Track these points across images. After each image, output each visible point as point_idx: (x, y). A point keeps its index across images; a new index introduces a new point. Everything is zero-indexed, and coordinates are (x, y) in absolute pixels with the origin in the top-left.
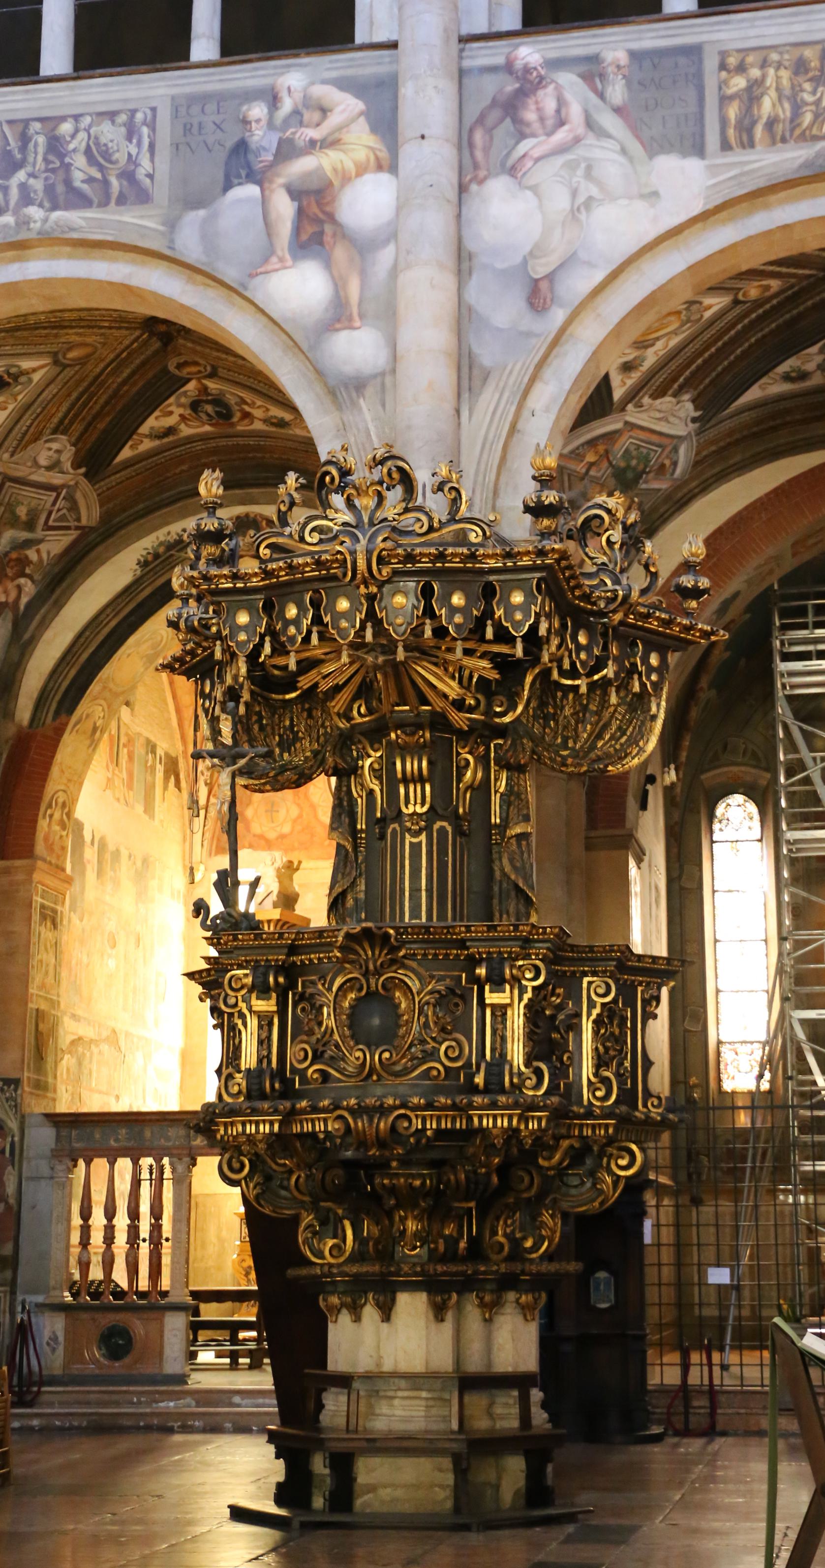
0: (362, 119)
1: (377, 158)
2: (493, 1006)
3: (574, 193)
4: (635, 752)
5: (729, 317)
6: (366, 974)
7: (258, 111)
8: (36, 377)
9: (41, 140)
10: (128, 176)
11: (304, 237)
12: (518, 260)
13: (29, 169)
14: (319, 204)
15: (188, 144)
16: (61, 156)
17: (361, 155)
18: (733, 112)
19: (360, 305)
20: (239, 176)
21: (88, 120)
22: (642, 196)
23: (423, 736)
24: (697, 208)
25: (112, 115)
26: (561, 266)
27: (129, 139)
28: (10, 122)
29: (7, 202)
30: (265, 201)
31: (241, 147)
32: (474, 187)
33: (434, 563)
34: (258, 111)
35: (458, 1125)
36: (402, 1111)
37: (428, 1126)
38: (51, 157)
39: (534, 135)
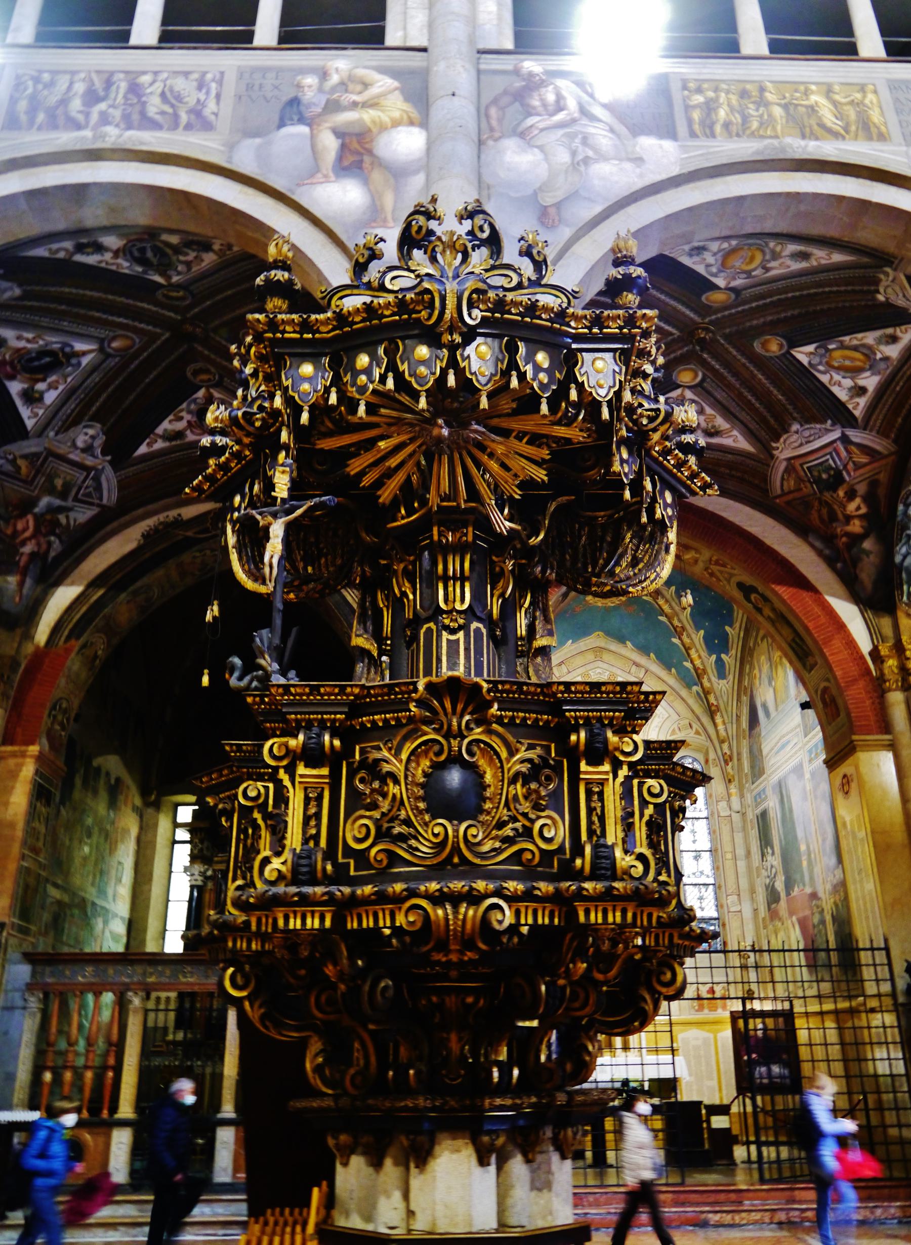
0: (397, 92)
1: (409, 117)
2: (588, 782)
3: (574, 153)
4: (653, 577)
7: (310, 80)
8: (85, 361)
9: (123, 86)
10: (197, 112)
11: (346, 163)
12: (530, 192)
13: (110, 102)
14: (359, 142)
15: (250, 96)
16: (139, 96)
17: (397, 114)
18: (696, 115)
19: (394, 211)
20: (292, 119)
21: (165, 75)
22: (630, 160)
23: (466, 535)
24: (675, 171)
25: (186, 74)
26: (566, 199)
27: (200, 88)
28: (98, 72)
29: (87, 123)
30: (313, 137)
31: (295, 102)
32: (491, 143)
33: (523, 317)
34: (310, 80)
37: (523, 921)
38: (130, 96)
39: (539, 115)
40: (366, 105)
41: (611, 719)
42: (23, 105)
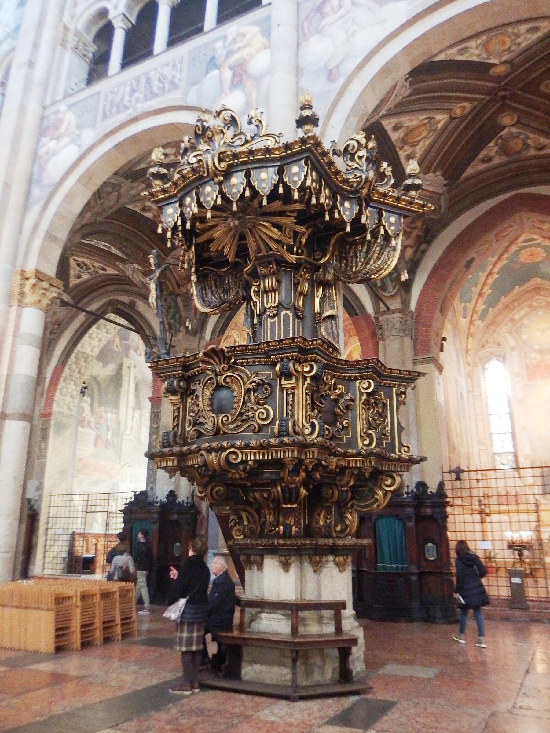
2: (287, 389)
4: (385, 267)
5: (450, 128)
6: (216, 375)
9: (143, 81)
10: (172, 83)
11: (235, 83)
23: (272, 268)
25: (167, 64)
26: (342, 61)
30: (220, 75)
31: (213, 59)
32: (304, 43)
35: (266, 458)
36: (232, 450)
37: (249, 458)
40: (245, 46)
41: (293, 356)
42: (108, 107)
